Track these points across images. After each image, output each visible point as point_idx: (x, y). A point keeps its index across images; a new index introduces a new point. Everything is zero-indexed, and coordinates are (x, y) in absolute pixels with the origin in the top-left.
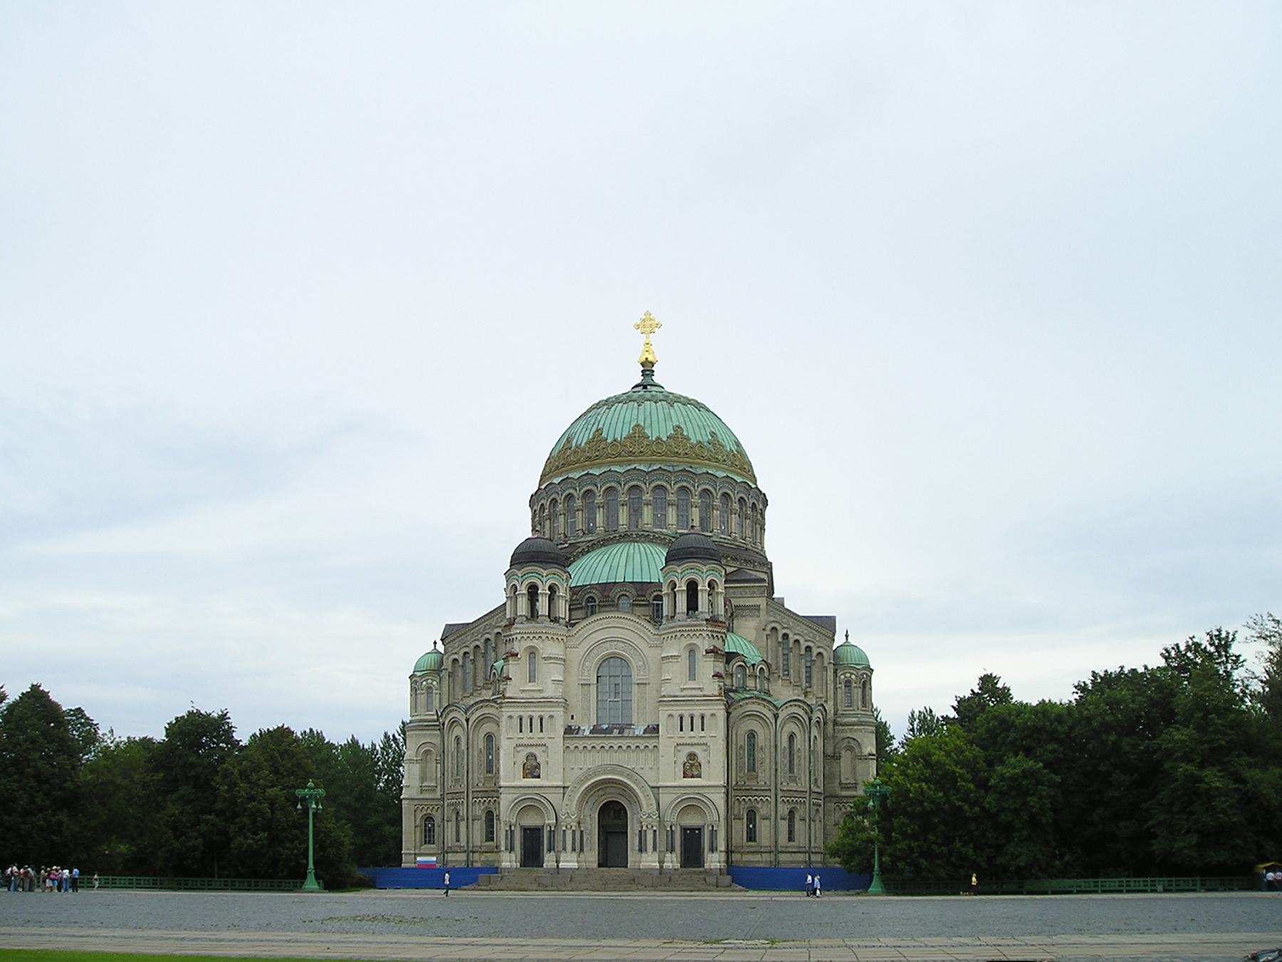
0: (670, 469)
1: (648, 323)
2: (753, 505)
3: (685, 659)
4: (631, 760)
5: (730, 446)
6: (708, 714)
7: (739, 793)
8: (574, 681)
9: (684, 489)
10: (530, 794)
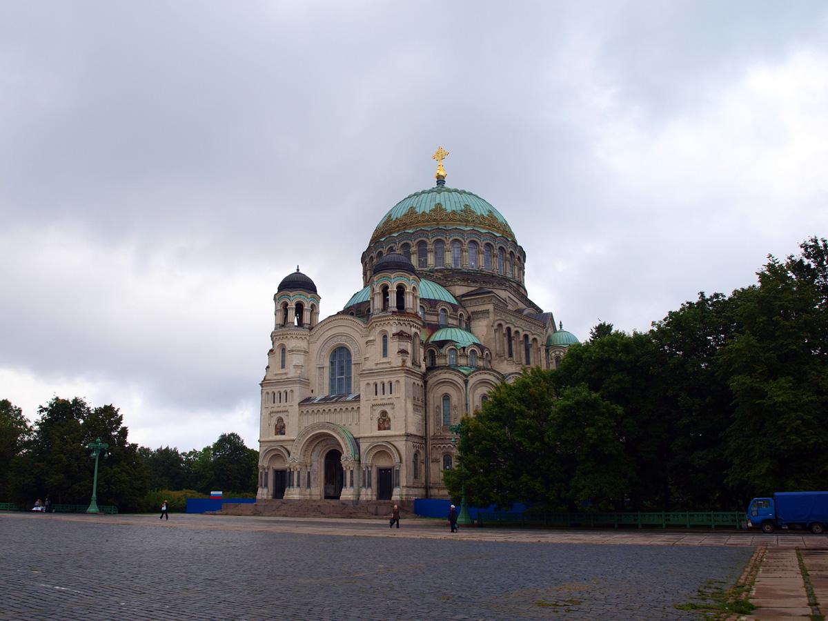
0: (429, 229)
1: (440, 155)
2: (518, 257)
3: (379, 340)
4: (338, 419)
5: (480, 211)
6: (393, 380)
7: (435, 441)
8: (314, 365)
9: (438, 241)
10: (275, 446)
